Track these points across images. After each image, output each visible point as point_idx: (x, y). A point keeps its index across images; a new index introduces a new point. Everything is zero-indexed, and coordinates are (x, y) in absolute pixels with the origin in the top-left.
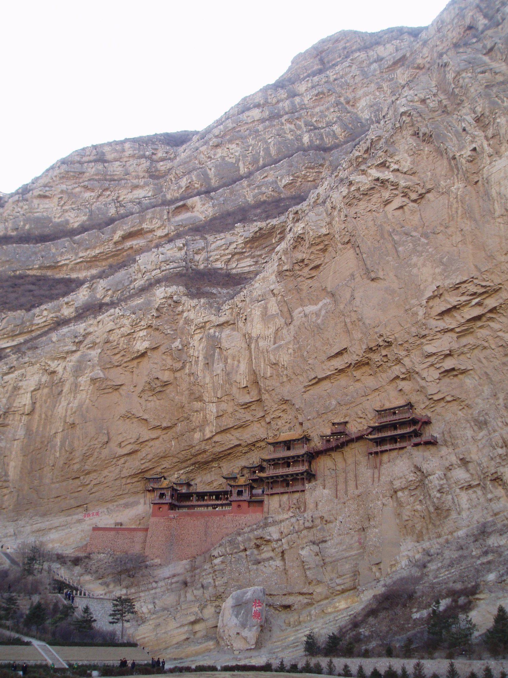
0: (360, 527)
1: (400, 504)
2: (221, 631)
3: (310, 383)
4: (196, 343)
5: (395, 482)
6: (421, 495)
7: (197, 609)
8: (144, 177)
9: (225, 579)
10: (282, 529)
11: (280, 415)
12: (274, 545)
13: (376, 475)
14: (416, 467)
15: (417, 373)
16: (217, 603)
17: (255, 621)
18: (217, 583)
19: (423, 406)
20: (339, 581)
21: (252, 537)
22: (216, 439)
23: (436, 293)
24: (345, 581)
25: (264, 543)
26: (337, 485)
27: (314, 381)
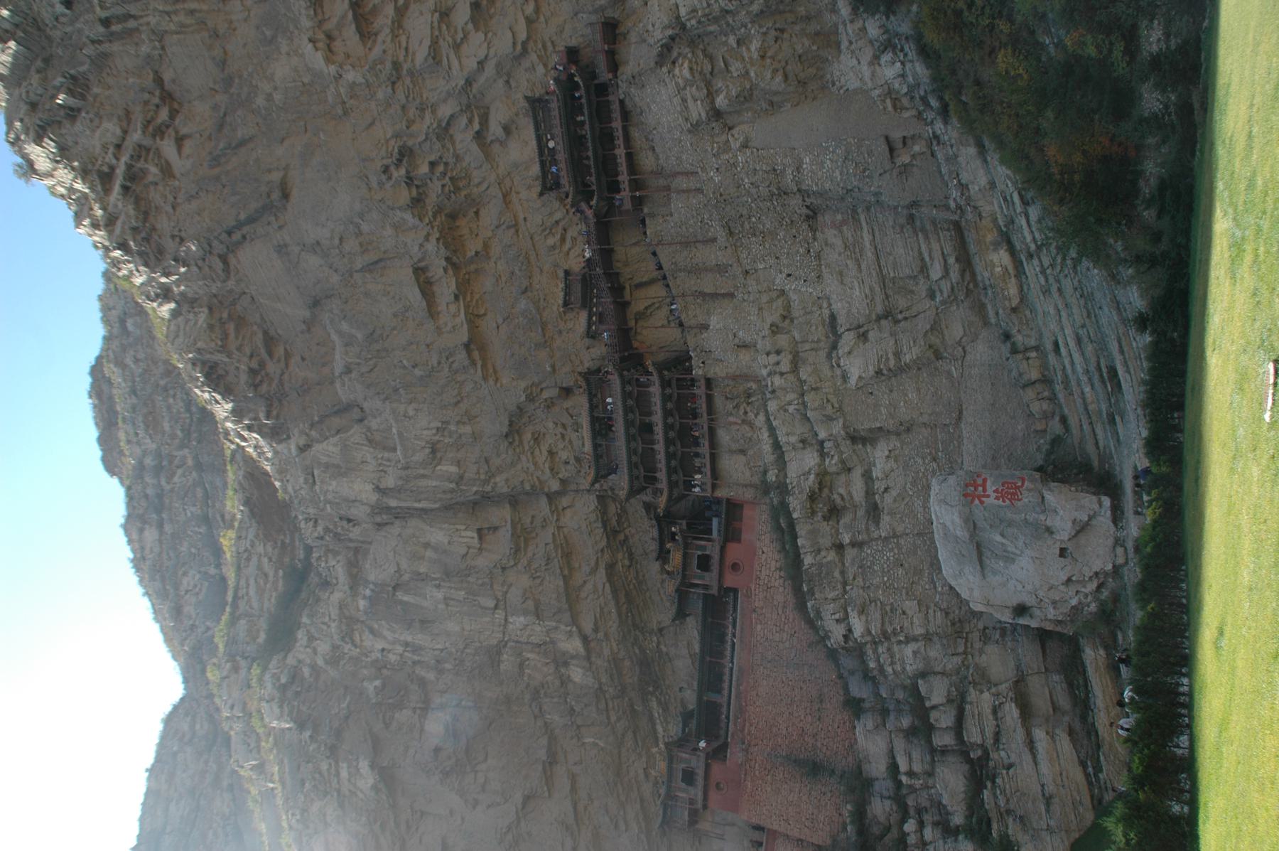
0: (805, 226)
1: (746, 97)
2: (1051, 613)
3: (479, 364)
4: (379, 646)
5: (694, 116)
6: (725, 43)
7: (986, 695)
8: (206, 762)
9: (910, 606)
10: (793, 439)
11: (546, 453)
12: (832, 464)
13: (682, 183)
14: (659, 64)
15: (469, 82)
16: (975, 636)
17: (1027, 498)
18: (919, 631)
19: (540, 69)
20: (936, 272)
21: (809, 527)
22: (588, 626)
23: (320, 45)
24: (937, 254)
25: (826, 491)
26: (703, 295)
27: (476, 354)
